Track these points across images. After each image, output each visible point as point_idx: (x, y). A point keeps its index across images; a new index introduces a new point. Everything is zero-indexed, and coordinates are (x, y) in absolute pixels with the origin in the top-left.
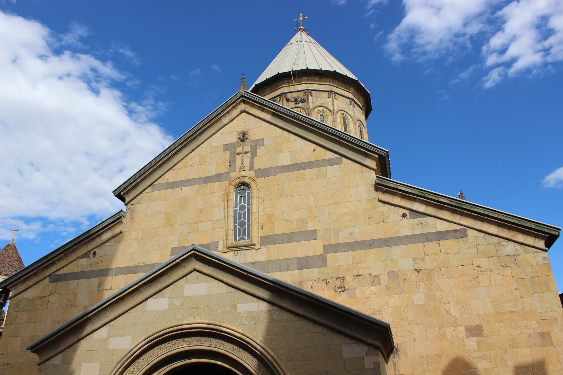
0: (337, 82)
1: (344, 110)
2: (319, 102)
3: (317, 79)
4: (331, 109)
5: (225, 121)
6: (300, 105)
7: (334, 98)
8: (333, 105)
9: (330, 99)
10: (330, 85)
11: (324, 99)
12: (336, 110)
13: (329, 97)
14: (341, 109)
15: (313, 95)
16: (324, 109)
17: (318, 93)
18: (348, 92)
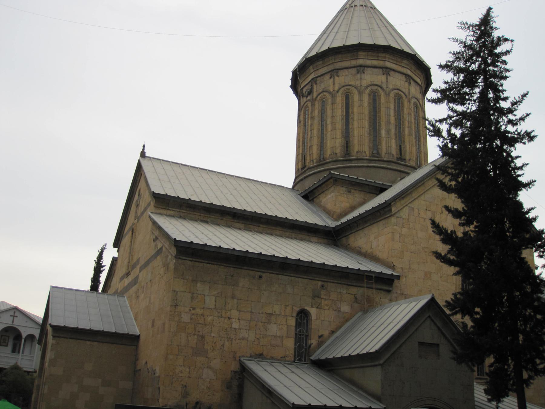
0: (340, 56)
1: (347, 84)
2: (322, 86)
3: (321, 62)
4: (332, 90)
5: (138, 181)
6: (309, 98)
7: (335, 76)
8: (334, 84)
9: (332, 80)
10: (332, 63)
11: (327, 83)
12: (336, 89)
13: (331, 78)
14: (343, 84)
15: (318, 82)
16: (325, 93)
17: (322, 77)
18: (356, 59)
